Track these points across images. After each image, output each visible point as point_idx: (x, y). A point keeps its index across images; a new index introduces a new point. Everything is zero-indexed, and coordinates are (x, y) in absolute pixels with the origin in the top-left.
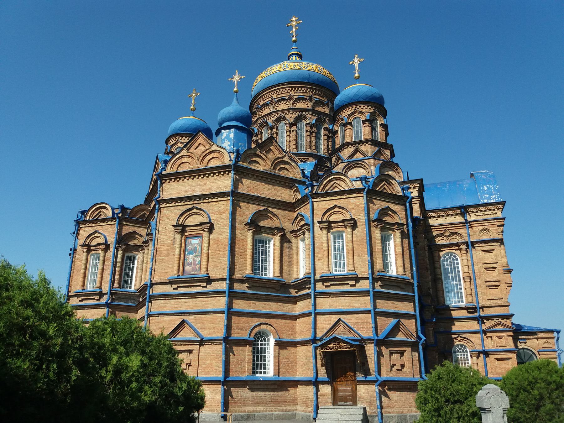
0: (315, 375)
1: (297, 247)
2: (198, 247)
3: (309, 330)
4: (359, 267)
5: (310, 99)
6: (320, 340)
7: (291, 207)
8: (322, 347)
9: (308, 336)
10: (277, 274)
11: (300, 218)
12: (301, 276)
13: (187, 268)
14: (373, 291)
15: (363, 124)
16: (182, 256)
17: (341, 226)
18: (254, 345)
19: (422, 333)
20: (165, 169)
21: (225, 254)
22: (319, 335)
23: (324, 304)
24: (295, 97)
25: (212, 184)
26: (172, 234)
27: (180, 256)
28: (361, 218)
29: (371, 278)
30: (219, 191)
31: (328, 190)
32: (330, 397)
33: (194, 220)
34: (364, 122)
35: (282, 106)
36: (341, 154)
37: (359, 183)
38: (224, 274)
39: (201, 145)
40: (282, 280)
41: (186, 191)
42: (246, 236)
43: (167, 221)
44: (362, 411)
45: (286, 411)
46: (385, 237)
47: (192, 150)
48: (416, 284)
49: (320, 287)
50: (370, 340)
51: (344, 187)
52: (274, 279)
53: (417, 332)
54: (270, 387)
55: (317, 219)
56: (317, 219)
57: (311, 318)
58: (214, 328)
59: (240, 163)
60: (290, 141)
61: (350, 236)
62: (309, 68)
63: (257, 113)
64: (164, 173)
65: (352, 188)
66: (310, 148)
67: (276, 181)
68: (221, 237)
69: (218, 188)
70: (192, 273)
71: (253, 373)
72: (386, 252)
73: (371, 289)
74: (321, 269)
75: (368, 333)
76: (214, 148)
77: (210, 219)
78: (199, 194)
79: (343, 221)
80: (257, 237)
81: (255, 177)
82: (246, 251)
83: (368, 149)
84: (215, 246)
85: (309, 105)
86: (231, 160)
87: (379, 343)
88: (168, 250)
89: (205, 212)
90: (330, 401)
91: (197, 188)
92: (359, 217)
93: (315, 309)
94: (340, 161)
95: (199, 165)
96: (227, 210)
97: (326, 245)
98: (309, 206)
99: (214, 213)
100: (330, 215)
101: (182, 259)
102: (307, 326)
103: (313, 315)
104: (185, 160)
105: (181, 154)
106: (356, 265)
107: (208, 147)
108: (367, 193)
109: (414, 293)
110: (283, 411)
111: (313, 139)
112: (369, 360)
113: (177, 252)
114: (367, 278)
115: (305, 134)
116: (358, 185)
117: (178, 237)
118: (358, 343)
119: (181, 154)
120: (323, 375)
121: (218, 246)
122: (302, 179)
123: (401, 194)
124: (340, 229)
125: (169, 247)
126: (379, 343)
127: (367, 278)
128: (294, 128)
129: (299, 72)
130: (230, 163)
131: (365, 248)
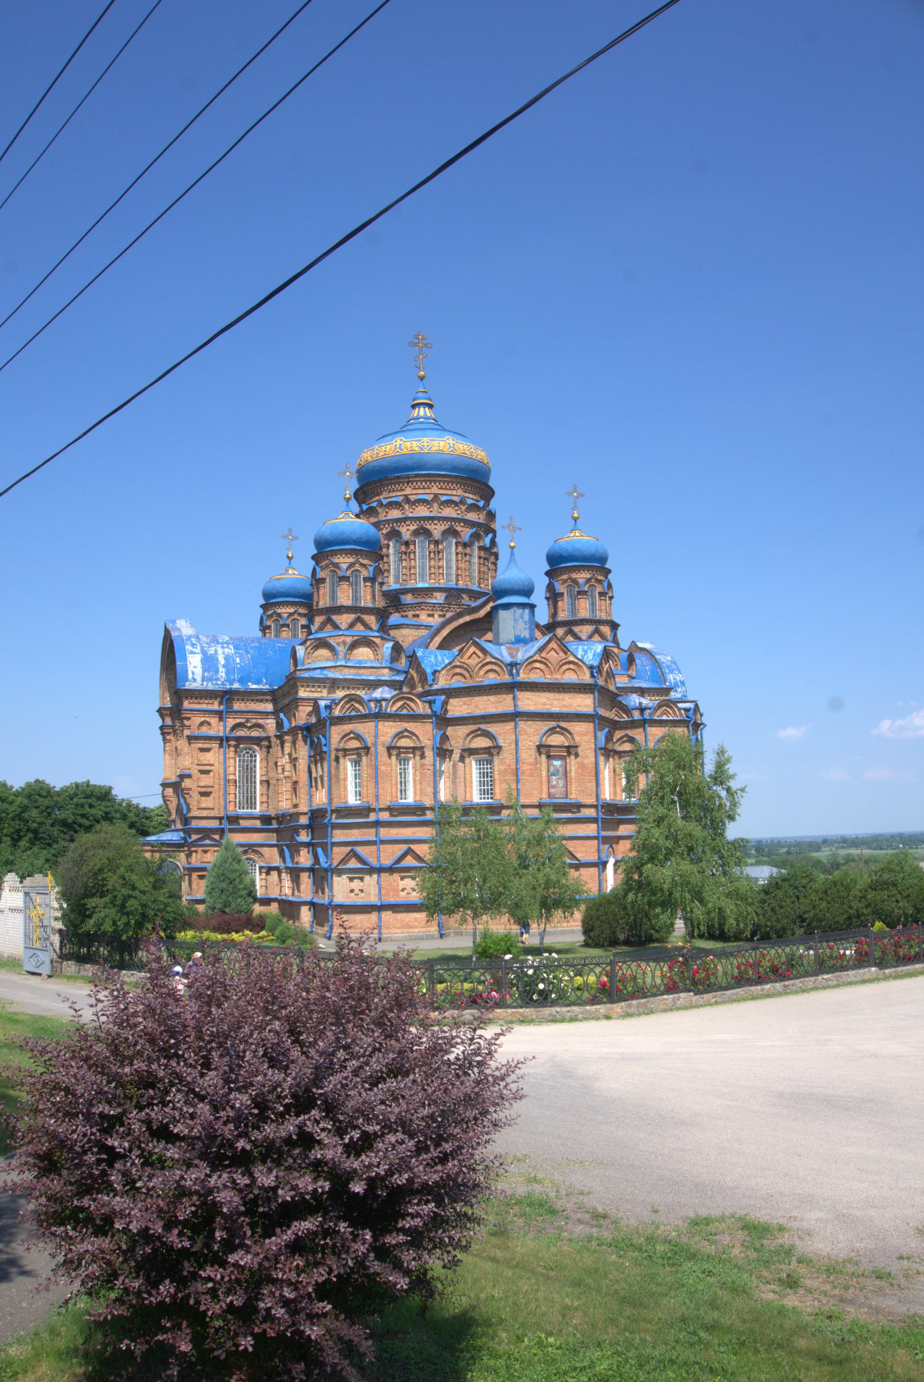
25: (570, 701)
33: (557, 740)
36: (576, 629)
41: (544, 704)
43: (525, 737)
47: (544, 654)
68: (586, 762)
69: (579, 706)
76: (571, 658)
89: (570, 733)
91: (556, 702)
104: (537, 665)
107: (562, 654)
115: (476, 560)
119: (535, 658)
128: (468, 551)
129: (469, 461)
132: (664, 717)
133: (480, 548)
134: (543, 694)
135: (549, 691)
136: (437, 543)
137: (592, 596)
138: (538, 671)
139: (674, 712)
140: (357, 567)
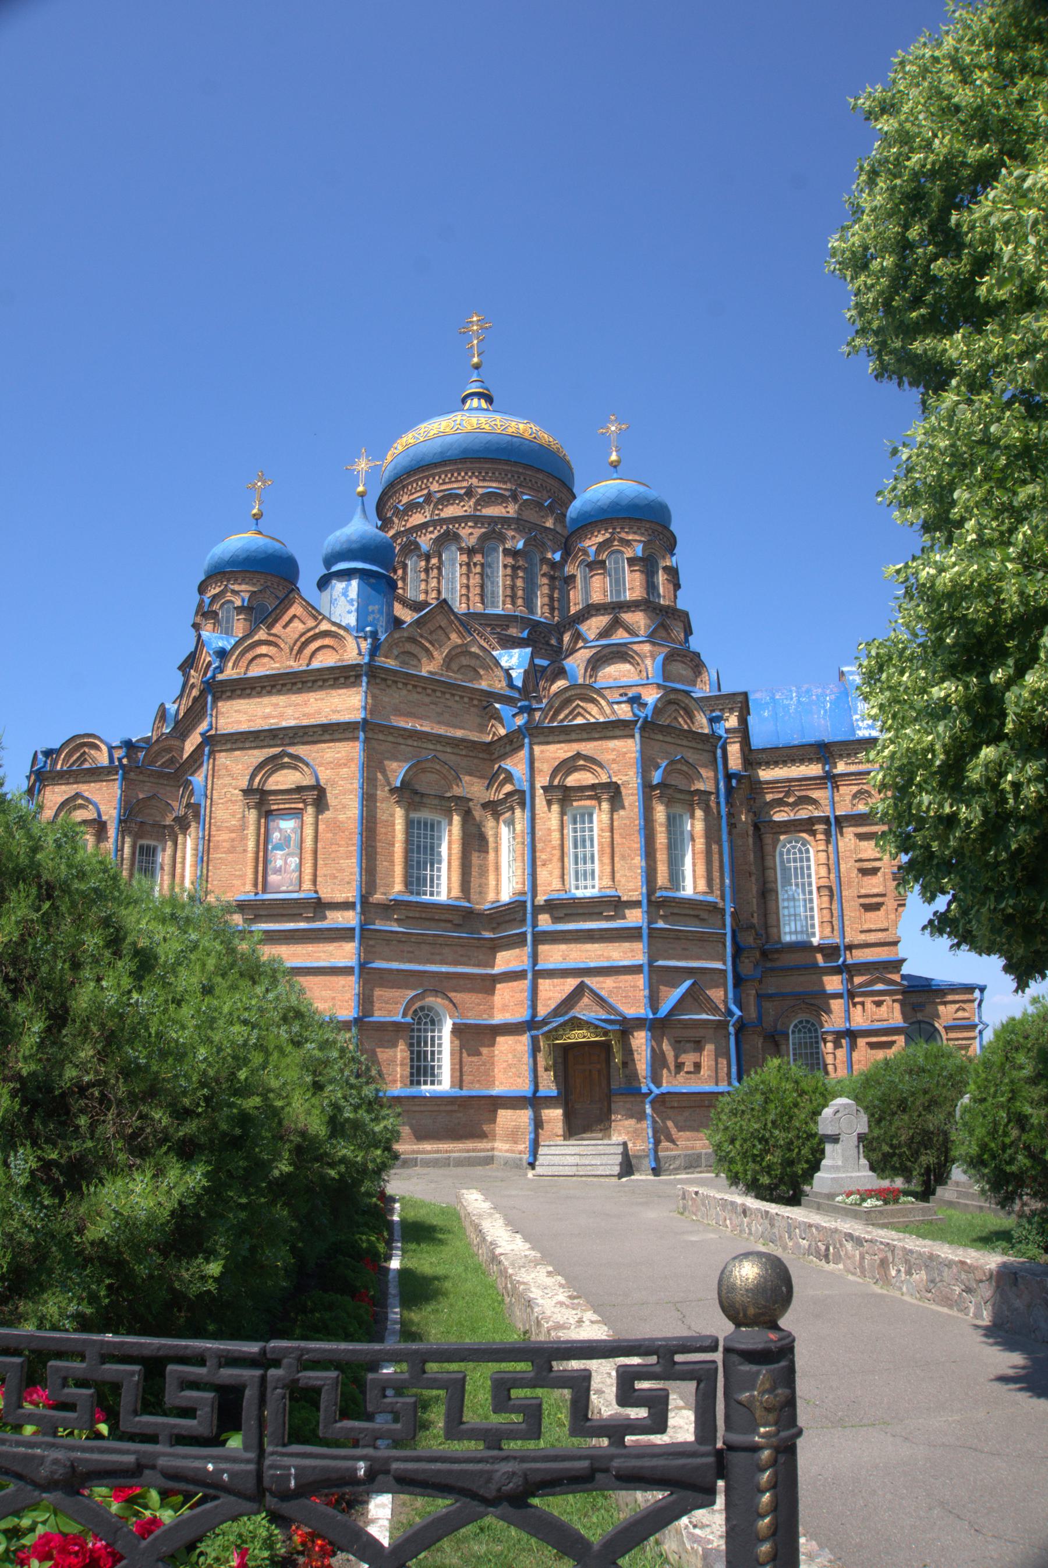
0: (532, 1088)
1: (497, 835)
2: (293, 836)
3: (520, 1003)
4: (623, 880)
5: (515, 497)
6: (545, 1022)
7: (484, 751)
8: (547, 1035)
9: (521, 1015)
10: (456, 892)
11: (502, 776)
12: (505, 897)
13: (273, 878)
14: (649, 928)
15: (630, 566)
16: (261, 854)
17: (590, 798)
18: (413, 1030)
19: (735, 1003)
20: (221, 669)
21: (351, 852)
22: (542, 1012)
23: (554, 956)
24: (480, 491)
25: (319, 704)
26: (238, 808)
27: (257, 853)
28: (630, 781)
29: (645, 902)
30: (336, 718)
31: (562, 721)
32: (560, 1124)
33: (284, 779)
34: (632, 561)
35: (451, 511)
36: (583, 628)
37: (625, 707)
38: (350, 893)
39: (296, 620)
40: (467, 904)
41: (266, 717)
42: (392, 815)
43: (227, 780)
44: (620, 1149)
45: (474, 1150)
46: (674, 818)
47: (277, 629)
48: (729, 909)
49: (545, 922)
50: (639, 1023)
51: (595, 714)
52: (450, 902)
53: (725, 1002)
54: (443, 1108)
55: (542, 781)
56: (542, 781)
57: (526, 983)
58: (333, 998)
59: (381, 661)
60: (468, 587)
61: (605, 817)
62: (510, 431)
63: (396, 520)
64: (220, 677)
65: (613, 718)
66: (513, 603)
67: (453, 695)
68: (342, 817)
69: (334, 711)
70: (284, 888)
71: (412, 1083)
72: (676, 849)
73: (645, 926)
74: (549, 885)
75: (635, 1007)
76: (325, 626)
77: (317, 780)
78: (292, 723)
79: (593, 787)
80: (414, 815)
81: (410, 687)
82: (393, 845)
83: (638, 619)
84: (330, 835)
85: (510, 510)
86: (360, 654)
87: (658, 1027)
88: (233, 840)
89: (307, 765)
90: (560, 1132)
91: (290, 711)
92: (625, 778)
93: (535, 962)
94: (580, 644)
95: (292, 663)
96: (352, 759)
97: (556, 835)
98: (524, 753)
99: (328, 765)
100: (568, 773)
101: (261, 859)
102: (518, 995)
103: (530, 976)
104: (263, 649)
105: (256, 638)
106: (617, 876)
107: (311, 623)
108: (643, 729)
109: (724, 926)
110: (468, 1151)
111: (519, 583)
112: (636, 1056)
113: (251, 844)
114: (636, 904)
116: (624, 711)
117: (252, 815)
118: (617, 1027)
119: (256, 638)
120: (548, 1086)
121: (335, 834)
122: (508, 692)
123: (706, 731)
124: (588, 803)
125: (233, 835)
126: (658, 1027)
127: (636, 904)
128: (478, 558)
129: (490, 437)
130: (359, 660)
131: (636, 843)
132: (580, 721)
133: (507, 552)
134: (266, 700)
135: (280, 692)
136: (428, 557)
137: (616, 570)
138: (266, 660)
139: (601, 708)
140: (229, 596)
